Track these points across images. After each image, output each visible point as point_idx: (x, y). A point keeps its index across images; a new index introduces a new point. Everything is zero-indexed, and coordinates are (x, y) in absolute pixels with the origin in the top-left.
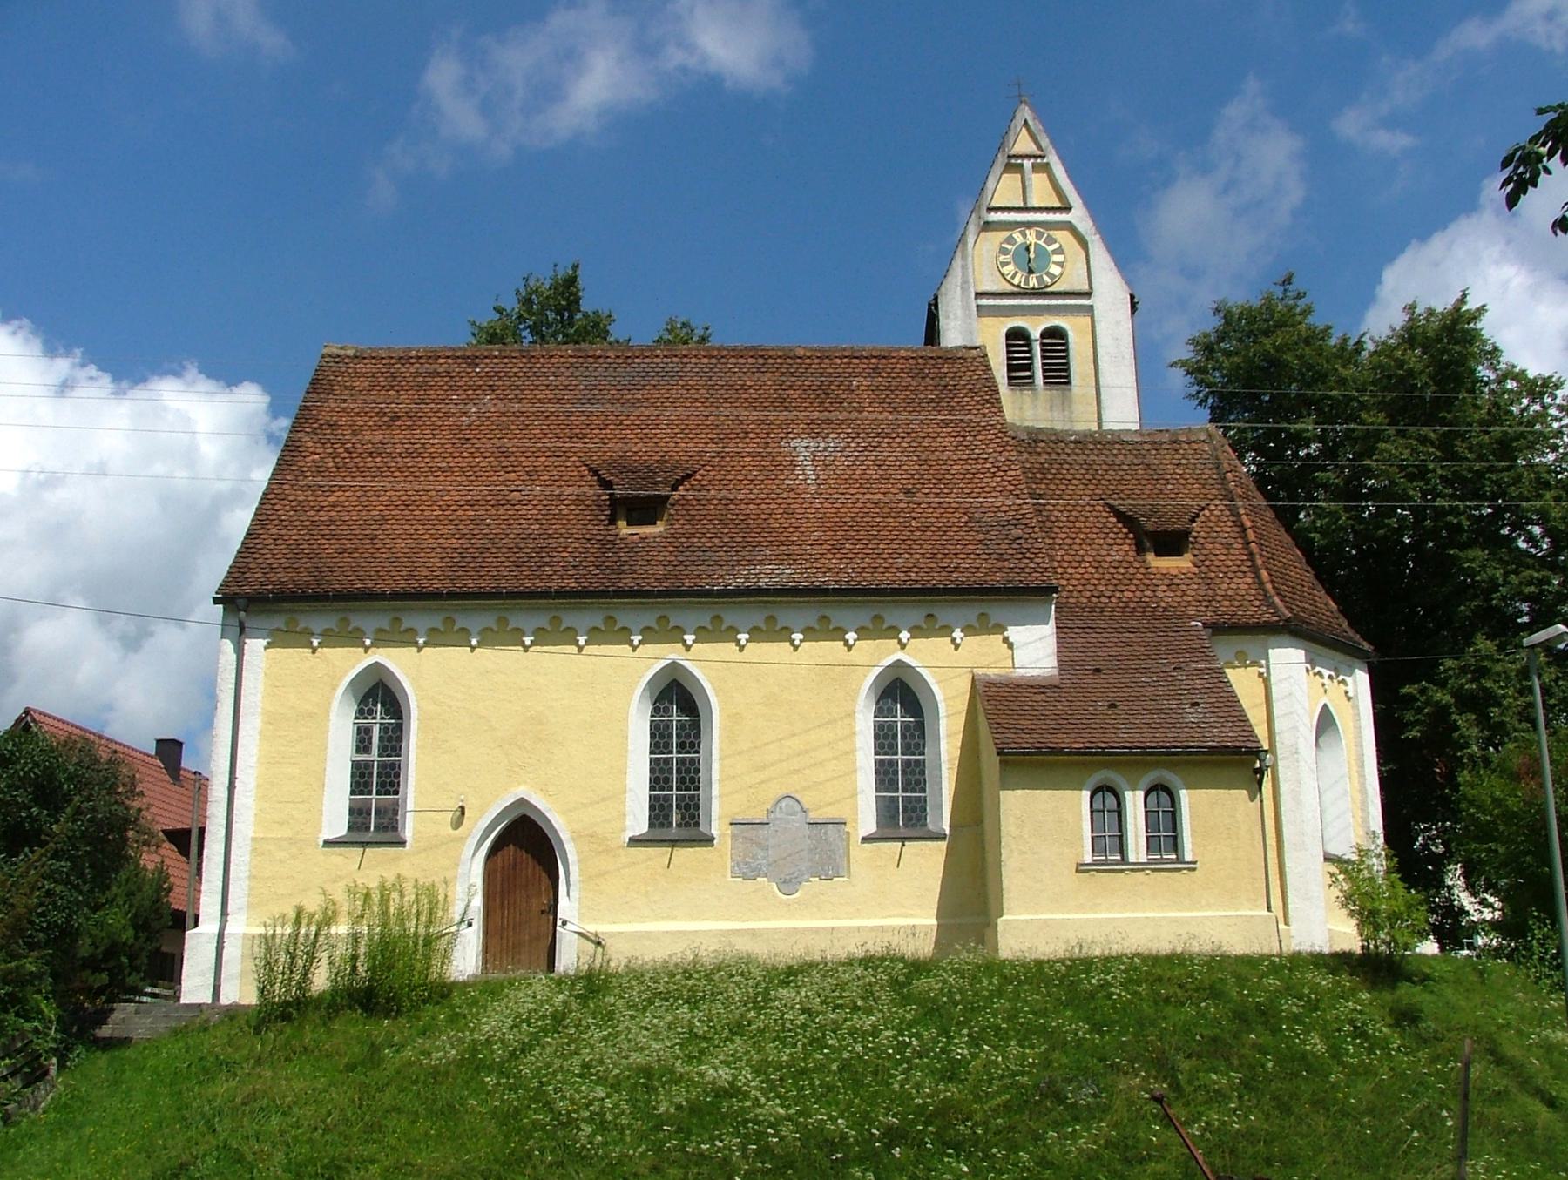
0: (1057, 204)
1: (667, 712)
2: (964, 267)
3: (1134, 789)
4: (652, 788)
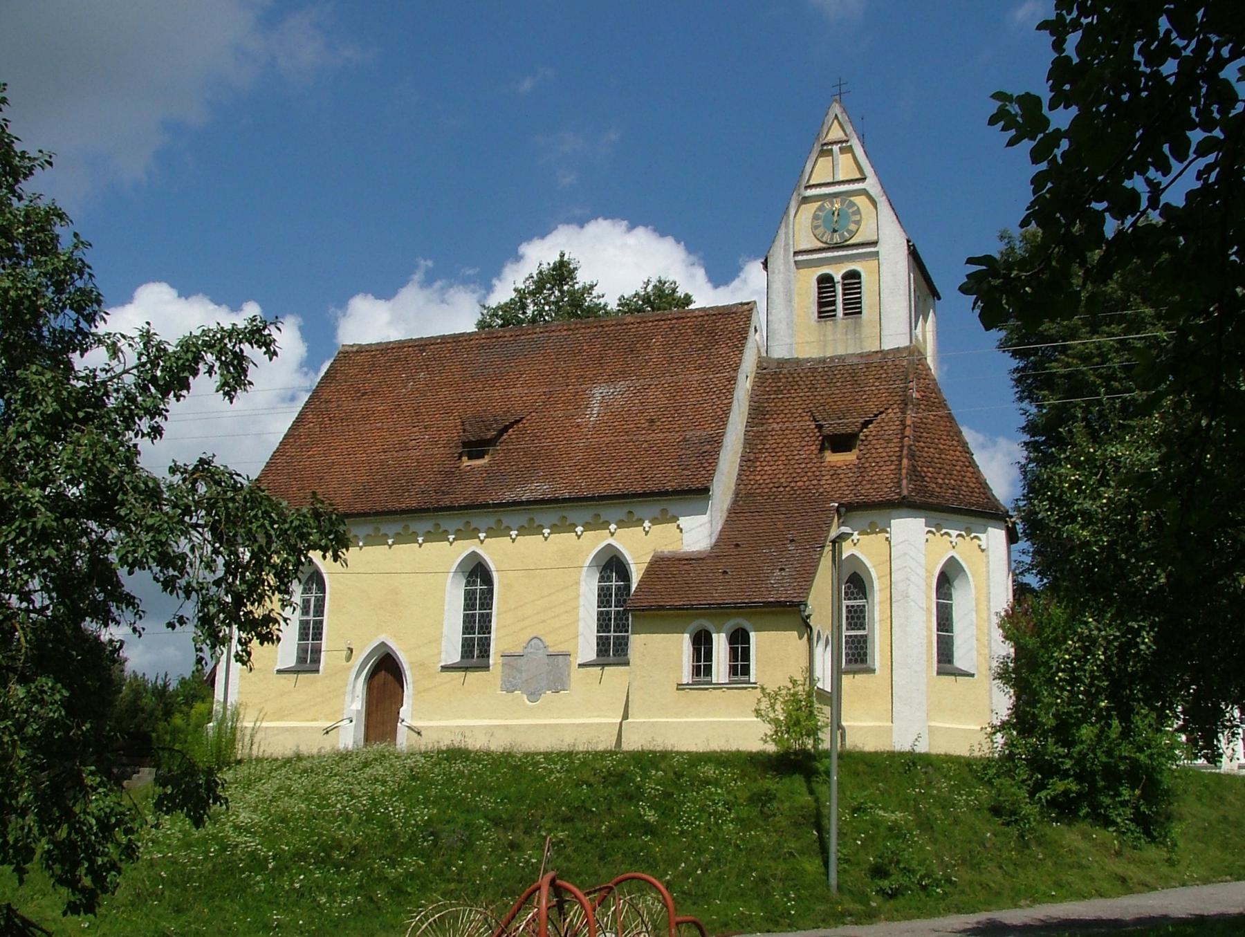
0: (858, 176)
1: (474, 583)
2: (787, 234)
3: (718, 632)
4: (464, 633)
